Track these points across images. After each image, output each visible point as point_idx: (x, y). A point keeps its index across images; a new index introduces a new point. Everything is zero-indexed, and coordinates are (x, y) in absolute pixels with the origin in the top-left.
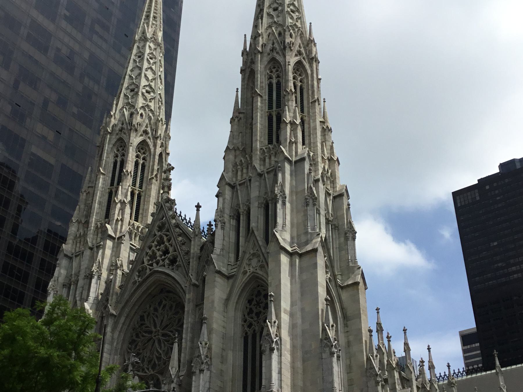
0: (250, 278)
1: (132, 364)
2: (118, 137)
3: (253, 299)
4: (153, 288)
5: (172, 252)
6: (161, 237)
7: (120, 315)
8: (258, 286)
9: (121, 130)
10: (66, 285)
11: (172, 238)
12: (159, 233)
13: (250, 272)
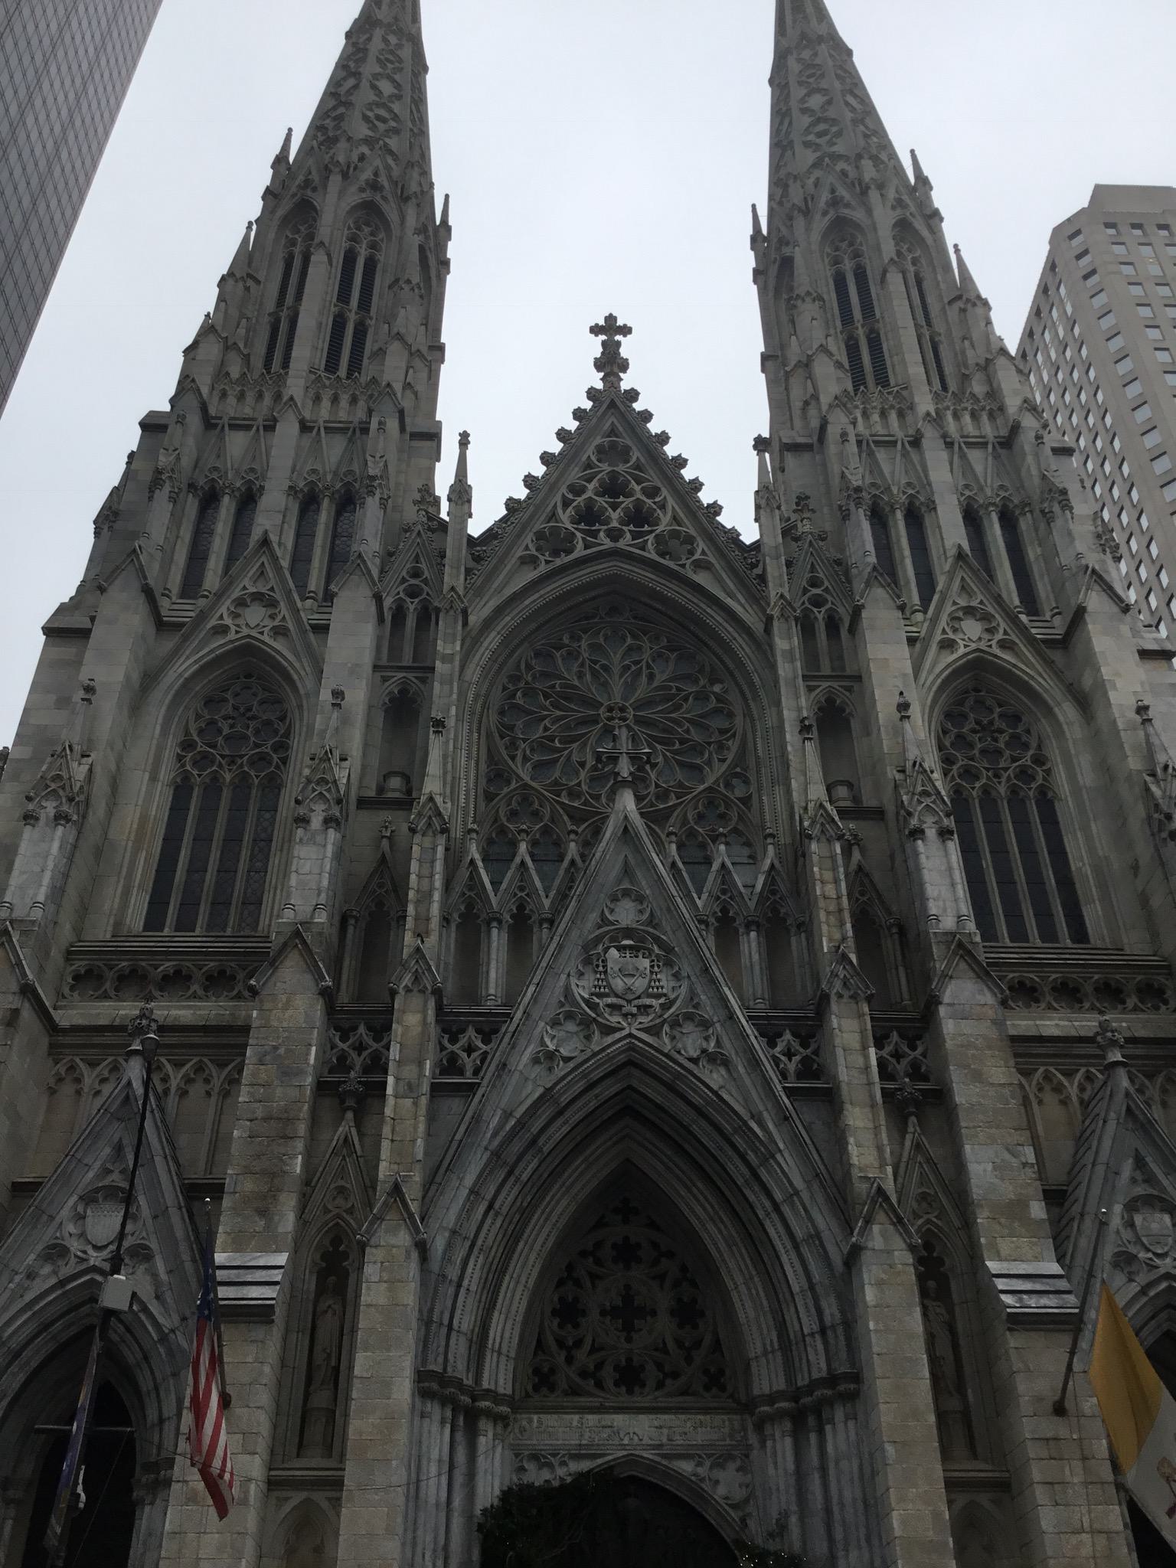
0: (968, 661)
1: (634, 758)
2: (366, 195)
3: (965, 717)
4: (593, 594)
5: (667, 525)
6: (614, 476)
8: (977, 690)
9: (374, 186)
10: (196, 489)
11: (665, 492)
12: (606, 467)
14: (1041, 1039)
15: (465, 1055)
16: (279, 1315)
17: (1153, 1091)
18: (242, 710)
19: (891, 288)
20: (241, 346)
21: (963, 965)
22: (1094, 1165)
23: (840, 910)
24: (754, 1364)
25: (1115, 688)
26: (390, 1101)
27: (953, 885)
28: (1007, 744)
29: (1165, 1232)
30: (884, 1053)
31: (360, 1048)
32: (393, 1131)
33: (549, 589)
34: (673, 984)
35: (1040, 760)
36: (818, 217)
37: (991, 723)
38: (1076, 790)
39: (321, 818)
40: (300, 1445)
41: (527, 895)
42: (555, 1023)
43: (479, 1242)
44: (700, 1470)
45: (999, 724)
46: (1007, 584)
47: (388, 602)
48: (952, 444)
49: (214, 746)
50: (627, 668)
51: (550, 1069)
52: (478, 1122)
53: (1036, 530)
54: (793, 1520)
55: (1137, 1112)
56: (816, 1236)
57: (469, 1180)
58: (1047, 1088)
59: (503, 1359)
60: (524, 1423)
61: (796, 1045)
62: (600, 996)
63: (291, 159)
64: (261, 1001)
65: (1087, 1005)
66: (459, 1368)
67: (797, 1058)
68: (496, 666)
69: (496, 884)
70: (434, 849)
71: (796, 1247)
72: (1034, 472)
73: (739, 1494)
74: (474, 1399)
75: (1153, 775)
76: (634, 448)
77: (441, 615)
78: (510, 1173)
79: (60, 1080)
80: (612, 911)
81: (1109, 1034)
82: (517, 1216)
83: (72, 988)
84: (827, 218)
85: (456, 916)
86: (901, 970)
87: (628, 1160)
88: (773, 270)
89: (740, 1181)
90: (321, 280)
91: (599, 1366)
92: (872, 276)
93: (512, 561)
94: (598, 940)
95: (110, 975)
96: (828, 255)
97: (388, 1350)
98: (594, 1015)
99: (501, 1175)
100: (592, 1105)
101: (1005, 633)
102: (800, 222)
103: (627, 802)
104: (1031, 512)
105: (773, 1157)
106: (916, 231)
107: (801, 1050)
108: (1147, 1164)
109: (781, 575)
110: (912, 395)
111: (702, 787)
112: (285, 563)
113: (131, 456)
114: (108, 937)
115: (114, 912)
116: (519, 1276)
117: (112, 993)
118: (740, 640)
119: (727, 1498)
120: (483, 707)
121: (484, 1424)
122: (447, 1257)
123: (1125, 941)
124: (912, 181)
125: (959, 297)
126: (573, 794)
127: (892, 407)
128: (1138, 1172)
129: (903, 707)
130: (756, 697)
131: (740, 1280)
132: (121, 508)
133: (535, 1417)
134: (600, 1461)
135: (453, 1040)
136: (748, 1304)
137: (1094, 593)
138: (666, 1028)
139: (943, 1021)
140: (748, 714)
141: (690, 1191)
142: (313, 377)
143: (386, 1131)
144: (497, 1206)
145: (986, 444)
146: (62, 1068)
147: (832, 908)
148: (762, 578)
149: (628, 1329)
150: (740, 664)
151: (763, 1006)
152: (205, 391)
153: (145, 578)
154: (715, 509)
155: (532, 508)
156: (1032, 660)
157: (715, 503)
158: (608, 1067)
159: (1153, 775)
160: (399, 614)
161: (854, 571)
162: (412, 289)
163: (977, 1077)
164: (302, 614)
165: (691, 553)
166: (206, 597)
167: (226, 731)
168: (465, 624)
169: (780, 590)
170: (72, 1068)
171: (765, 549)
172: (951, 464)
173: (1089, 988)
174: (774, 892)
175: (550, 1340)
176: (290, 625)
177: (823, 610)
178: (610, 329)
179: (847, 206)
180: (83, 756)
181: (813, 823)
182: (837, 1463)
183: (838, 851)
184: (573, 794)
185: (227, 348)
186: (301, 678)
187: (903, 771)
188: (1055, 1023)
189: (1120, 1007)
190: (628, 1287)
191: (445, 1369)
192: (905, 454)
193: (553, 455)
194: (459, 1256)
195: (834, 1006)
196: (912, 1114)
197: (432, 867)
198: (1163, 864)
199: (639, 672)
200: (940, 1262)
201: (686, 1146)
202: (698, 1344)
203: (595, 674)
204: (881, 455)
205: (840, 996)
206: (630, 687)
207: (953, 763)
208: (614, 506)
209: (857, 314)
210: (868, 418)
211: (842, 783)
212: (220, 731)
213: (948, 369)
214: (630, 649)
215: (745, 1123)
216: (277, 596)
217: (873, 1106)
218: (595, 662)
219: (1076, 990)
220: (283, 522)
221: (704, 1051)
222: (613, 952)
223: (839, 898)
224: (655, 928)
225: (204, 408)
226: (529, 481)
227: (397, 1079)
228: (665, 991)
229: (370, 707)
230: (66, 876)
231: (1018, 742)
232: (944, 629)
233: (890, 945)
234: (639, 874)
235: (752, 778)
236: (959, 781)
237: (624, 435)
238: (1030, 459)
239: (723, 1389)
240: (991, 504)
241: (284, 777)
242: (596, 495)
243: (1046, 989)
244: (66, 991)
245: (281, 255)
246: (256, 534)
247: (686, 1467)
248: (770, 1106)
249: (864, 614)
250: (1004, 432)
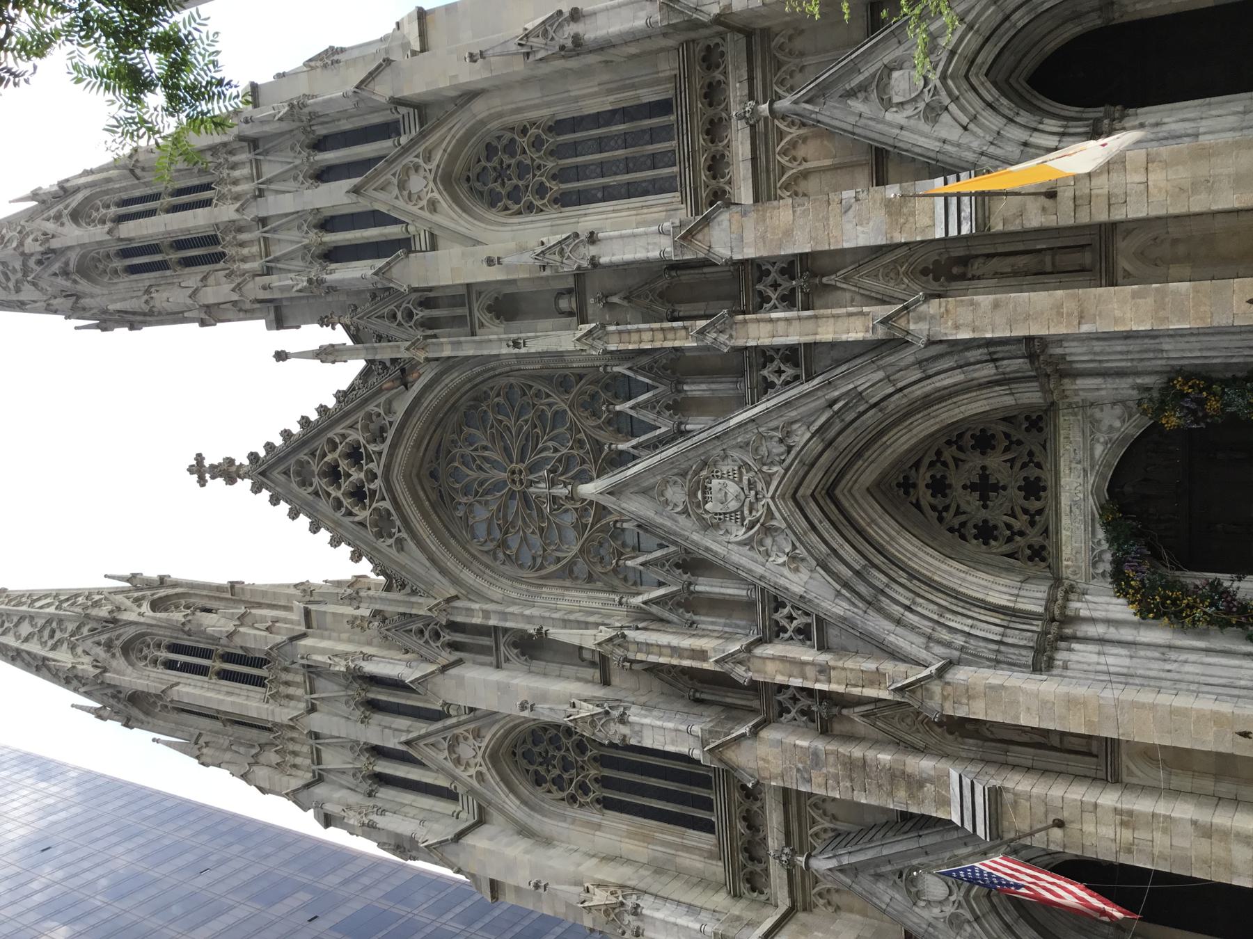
1: (553, 483)
2: (118, 652)
3: (491, 191)
4: (421, 494)
6: (323, 474)
7: (456, 581)
8: (468, 179)
9: (109, 646)
10: (373, 791)
11: (331, 435)
12: (316, 480)
13: (432, 191)
14: (754, 159)
15: (795, 622)
16: (996, 782)
17: (792, 64)
18: (541, 760)
19: (132, 235)
20: (254, 751)
21: (699, 236)
22: (854, 134)
23: (662, 329)
24: (1020, 402)
25: (456, 77)
26: (834, 687)
27: (634, 236)
28: (512, 155)
29: (907, 74)
30: (774, 297)
31: (794, 699)
32: (858, 686)
33: (421, 531)
34: (730, 461)
35: (524, 131)
36: (79, 288)
37: (495, 169)
38: (548, 105)
39: (621, 726)
40: (1090, 754)
41: (668, 561)
42: (768, 554)
43: (935, 617)
44: (1102, 440)
45: (495, 162)
46: (376, 150)
47: (447, 656)
48: (260, 190)
49: (571, 780)
50: (480, 468)
51: (803, 560)
52: (845, 619)
53: (327, 123)
54: (1139, 381)
55: (811, 94)
56: (920, 363)
57: (890, 626)
58: (793, 153)
59: (1022, 593)
60: (1069, 571)
61: (774, 366)
62: (743, 519)
63: (99, 706)
64: (764, 778)
65: (724, 115)
66: (1027, 639)
67: (782, 365)
68: (488, 571)
69: (661, 584)
71: (929, 377)
72: (277, 125)
73: (1118, 410)
74: (1053, 620)
75: (527, 55)
76: (297, 457)
77: (452, 618)
78: (882, 592)
79: (829, 903)
80: (676, 505)
81: (747, 115)
82: (915, 582)
83: (761, 892)
84: (78, 279)
85: (688, 616)
86: (706, 270)
87: (868, 489)
88: (131, 318)
89: (880, 414)
90: (192, 689)
91: (1025, 511)
92: (123, 246)
93: (402, 558)
94: (700, 519)
95: (751, 867)
96: (110, 279)
97: (1018, 702)
98: (759, 525)
99: (883, 599)
100: (827, 524)
101: (417, 156)
102: (86, 302)
103: (589, 490)
104: (310, 126)
105: (861, 393)
106: (79, 204)
107: (776, 363)
108: (852, 89)
109: (391, 347)
110: (222, 222)
111: (569, 413)
112: (422, 728)
113: (351, 834)
114: (721, 864)
115: (702, 859)
116: (959, 578)
117: (763, 865)
118: (447, 381)
119: (1124, 421)
120: (522, 582)
121: (1069, 613)
122: (948, 645)
123: (668, 73)
124: (35, 203)
125: (132, 171)
126: (583, 512)
127: (234, 238)
128: (859, 95)
129: (490, 261)
130: (493, 369)
131: (957, 411)
132: (393, 843)
133: (1065, 563)
134: (1097, 516)
135: (785, 631)
136: (974, 405)
137: (377, 88)
138: (765, 468)
139: (746, 257)
140: (507, 374)
141: (891, 445)
142: (271, 701)
143: (856, 691)
144: (907, 603)
145: (256, 160)
146: (822, 902)
147: (660, 335)
148: (394, 361)
149: (996, 487)
150: (470, 380)
151: (742, 385)
152: (295, 783)
153: (447, 840)
154: (341, 396)
155: (358, 542)
156: (438, 135)
157: (335, 396)
158: (799, 515)
159: (527, 55)
160: (454, 646)
161: (379, 286)
162: (189, 621)
163: (788, 233)
164: (463, 718)
165: (379, 415)
166: (455, 787)
167: (556, 772)
168: (456, 598)
169: (402, 349)
170: (820, 895)
171: (370, 357)
172: (278, 192)
173: (710, 112)
174: (651, 368)
175: (1006, 548)
176: (472, 726)
177: (415, 311)
178: (200, 470)
180: (588, 891)
181: (592, 347)
182: (1095, 354)
183: (612, 328)
184: (583, 512)
185: (257, 763)
186: (513, 720)
187: (544, 267)
188: (740, 144)
189: (723, 85)
190: (965, 487)
191: (1032, 647)
192: (274, 230)
193: (311, 523)
194: (945, 635)
195: (740, 343)
196: (821, 281)
197: (652, 645)
198: (602, 49)
199: (484, 457)
200: (936, 262)
201: (855, 450)
202: (1007, 436)
203: (487, 492)
204: (277, 251)
205: (731, 336)
206: (495, 464)
207: (531, 203)
209: (158, 258)
210: (247, 257)
211: (556, 304)
212: (560, 776)
213: (195, 181)
214: (465, 464)
215: (836, 413)
216: (449, 735)
217: (816, 317)
218: (477, 492)
219: (711, 122)
220: (390, 728)
221: (781, 441)
222: (708, 507)
223: (652, 330)
224: (687, 473)
225: (308, 786)
226: (335, 543)
227: (817, 681)
228: (736, 468)
229: (530, 672)
230: (679, 903)
231: (510, 148)
232: (421, 209)
233: (686, 277)
234: (645, 484)
235: (560, 372)
236: (546, 201)
237: (286, 465)
238: (267, 128)
239: (1040, 418)
240: (308, 159)
242: (339, 487)
243: (713, 149)
244: (763, 898)
245: (175, 716)
246: (404, 748)
247: (1099, 450)
248: (820, 393)
249: (415, 285)
250: (245, 144)
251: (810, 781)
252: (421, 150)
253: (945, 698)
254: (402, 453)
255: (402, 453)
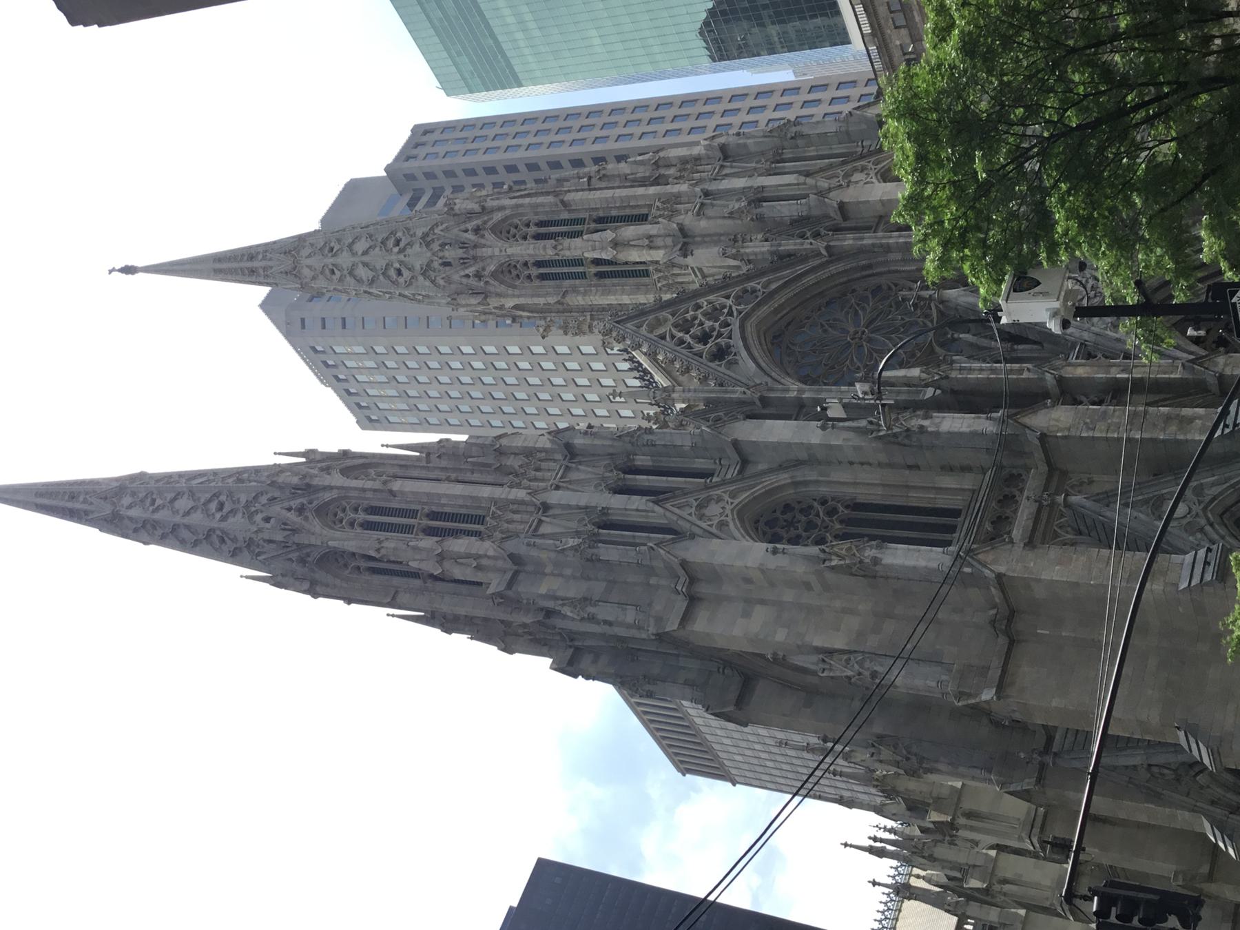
6: (676, 326)
64: (1051, 432)
70: (961, 369)
125: (590, 178)
127: (672, 206)
165: (754, 291)
179: (485, 223)
197: (974, 370)
208: (701, 324)
216: (703, 496)
218: (815, 345)
241: (847, 498)
251: (1094, 429)
252: (873, 159)
253: (1226, 365)
254: (765, 310)
255: (765, 310)
